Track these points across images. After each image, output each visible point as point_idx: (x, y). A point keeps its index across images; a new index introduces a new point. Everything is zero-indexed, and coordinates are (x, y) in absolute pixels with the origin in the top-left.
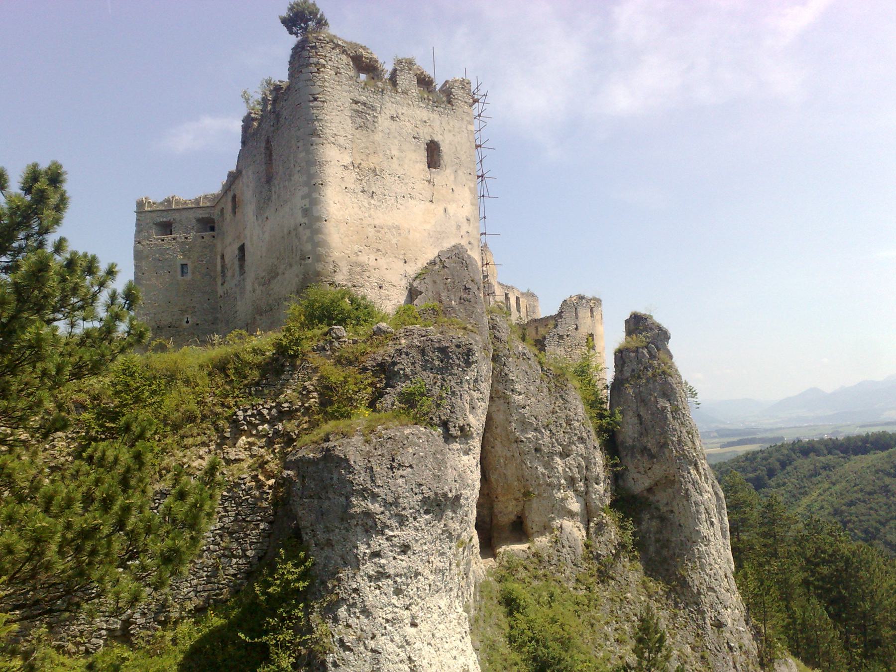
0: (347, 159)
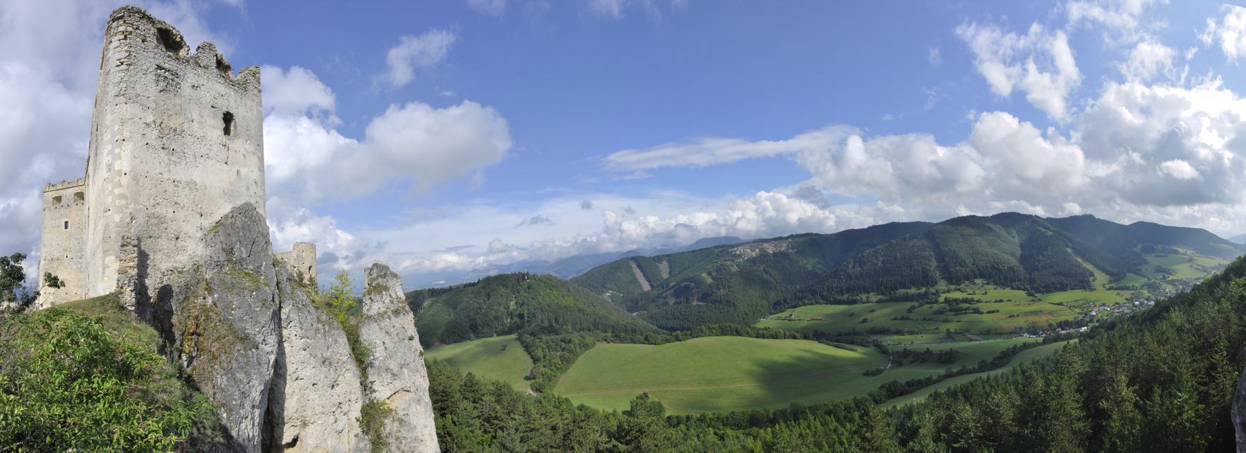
0: (150, 119)
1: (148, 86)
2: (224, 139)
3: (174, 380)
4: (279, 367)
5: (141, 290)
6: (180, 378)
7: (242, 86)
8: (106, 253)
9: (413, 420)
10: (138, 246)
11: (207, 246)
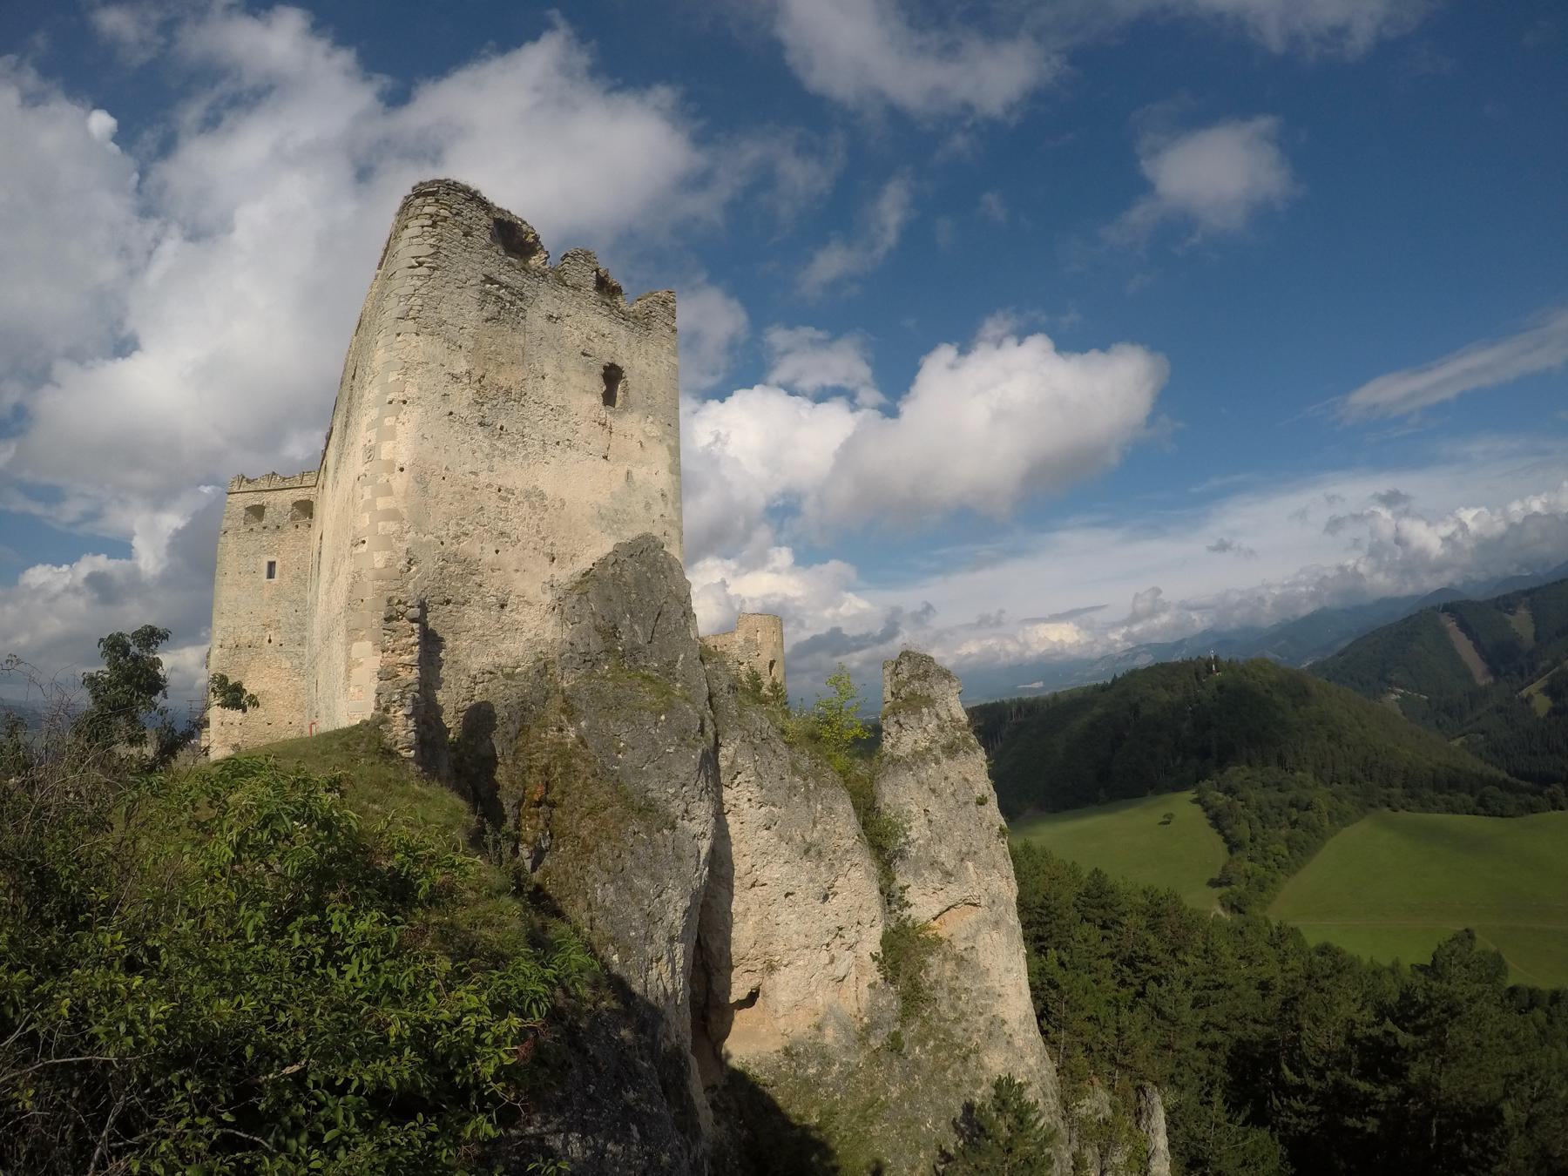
0: (461, 366)
1: (465, 310)
2: (604, 413)
3: (506, 900)
4: (720, 862)
5: (426, 714)
6: (518, 893)
7: (642, 322)
8: (353, 634)
9: (985, 959)
10: (421, 620)
11: (564, 620)
